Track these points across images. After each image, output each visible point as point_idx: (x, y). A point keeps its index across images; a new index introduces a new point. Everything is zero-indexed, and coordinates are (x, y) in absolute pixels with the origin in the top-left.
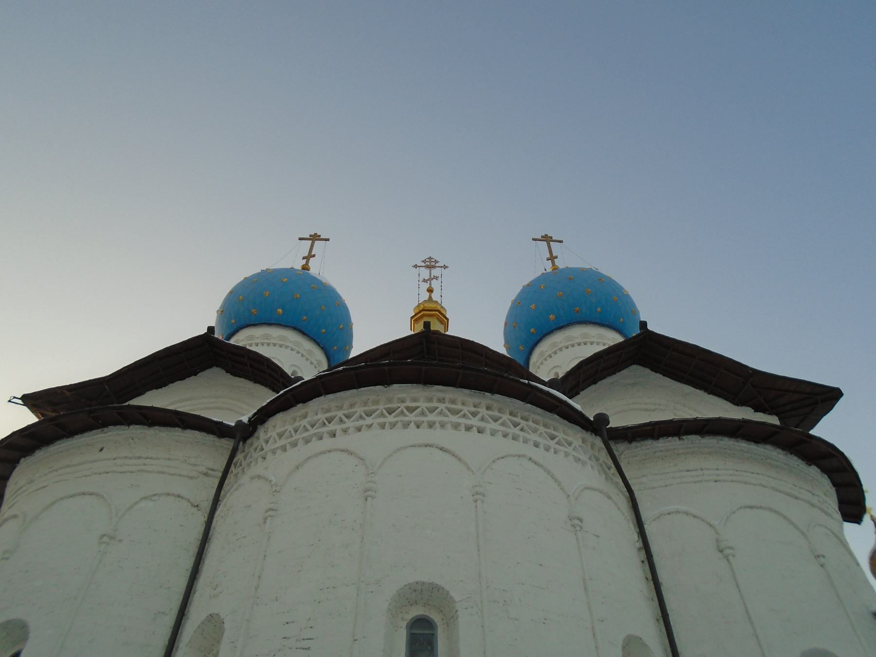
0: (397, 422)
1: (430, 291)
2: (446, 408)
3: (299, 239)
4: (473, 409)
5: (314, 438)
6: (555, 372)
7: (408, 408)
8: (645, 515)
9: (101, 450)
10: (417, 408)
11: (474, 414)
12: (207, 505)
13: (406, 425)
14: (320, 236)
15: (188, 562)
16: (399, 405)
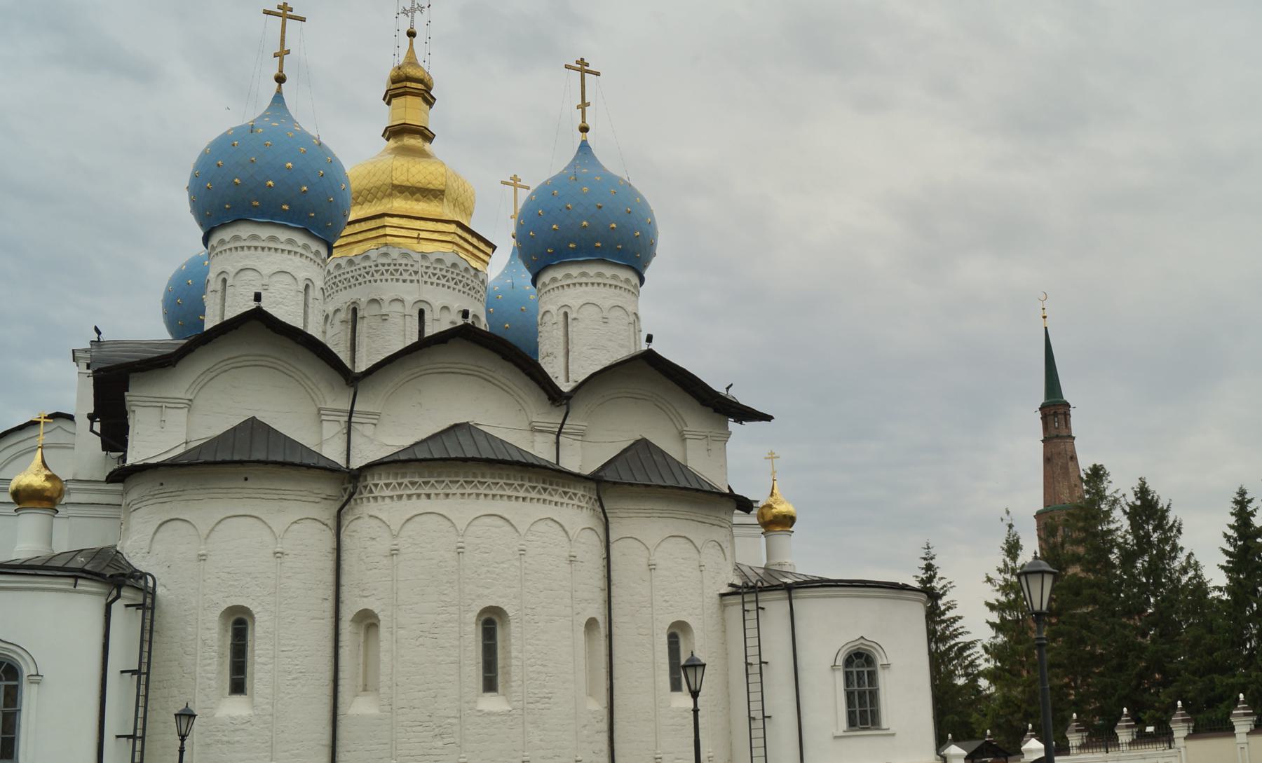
0: (472, 494)
1: (411, 34)
2: (505, 483)
3: (264, 13)
4: (520, 483)
5: (415, 496)
6: (566, 310)
7: (479, 482)
8: (613, 537)
9: (246, 479)
10: (486, 482)
11: (521, 486)
12: (332, 522)
13: (478, 495)
14: (291, 10)
15: (330, 564)
16: (473, 479)
